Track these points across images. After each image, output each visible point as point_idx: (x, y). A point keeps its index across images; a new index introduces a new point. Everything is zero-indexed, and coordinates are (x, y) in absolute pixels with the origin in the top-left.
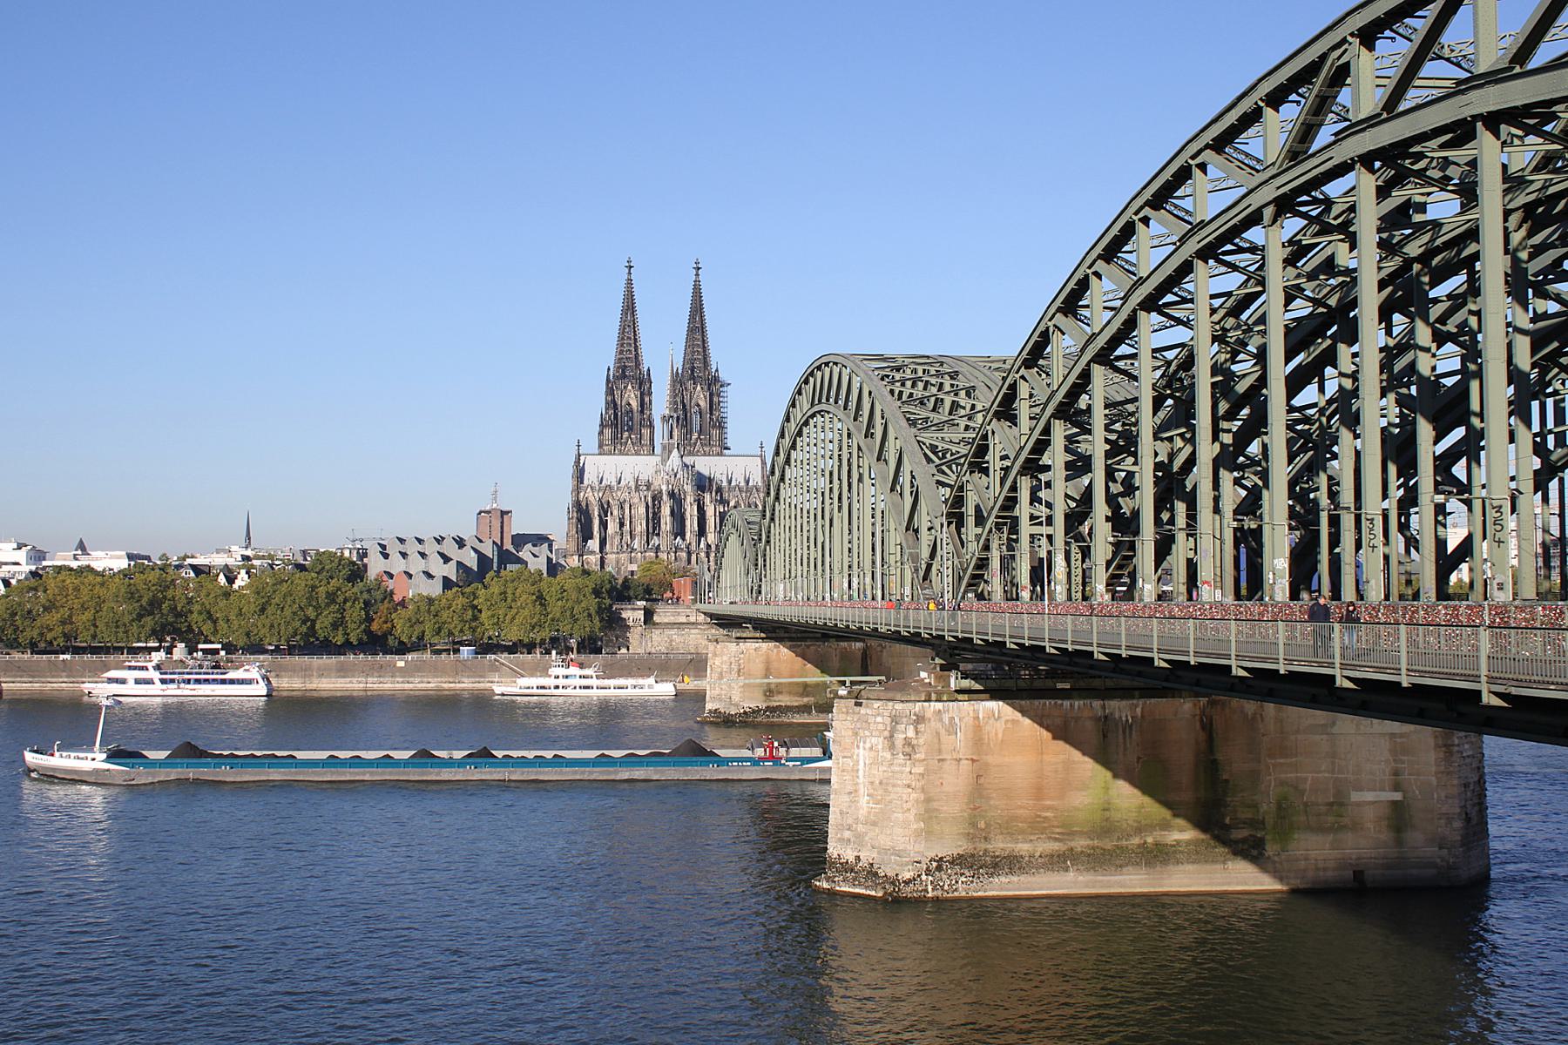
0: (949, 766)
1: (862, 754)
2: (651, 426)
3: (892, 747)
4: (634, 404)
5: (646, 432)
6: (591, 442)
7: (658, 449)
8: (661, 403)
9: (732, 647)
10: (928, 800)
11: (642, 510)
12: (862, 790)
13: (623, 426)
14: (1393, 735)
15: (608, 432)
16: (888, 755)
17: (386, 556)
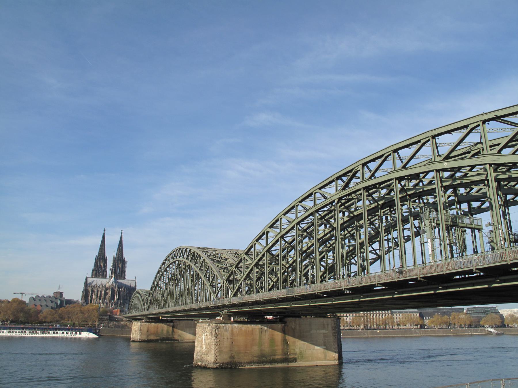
0: (225, 340)
1: (204, 337)
2: (106, 272)
3: (212, 335)
4: (102, 265)
5: (105, 273)
6: (90, 275)
7: (108, 277)
8: (110, 265)
9: (139, 323)
10: (220, 348)
11: (103, 292)
12: (204, 346)
13: (99, 270)
14: (324, 333)
15: (95, 273)
16: (210, 337)
17: (35, 300)
